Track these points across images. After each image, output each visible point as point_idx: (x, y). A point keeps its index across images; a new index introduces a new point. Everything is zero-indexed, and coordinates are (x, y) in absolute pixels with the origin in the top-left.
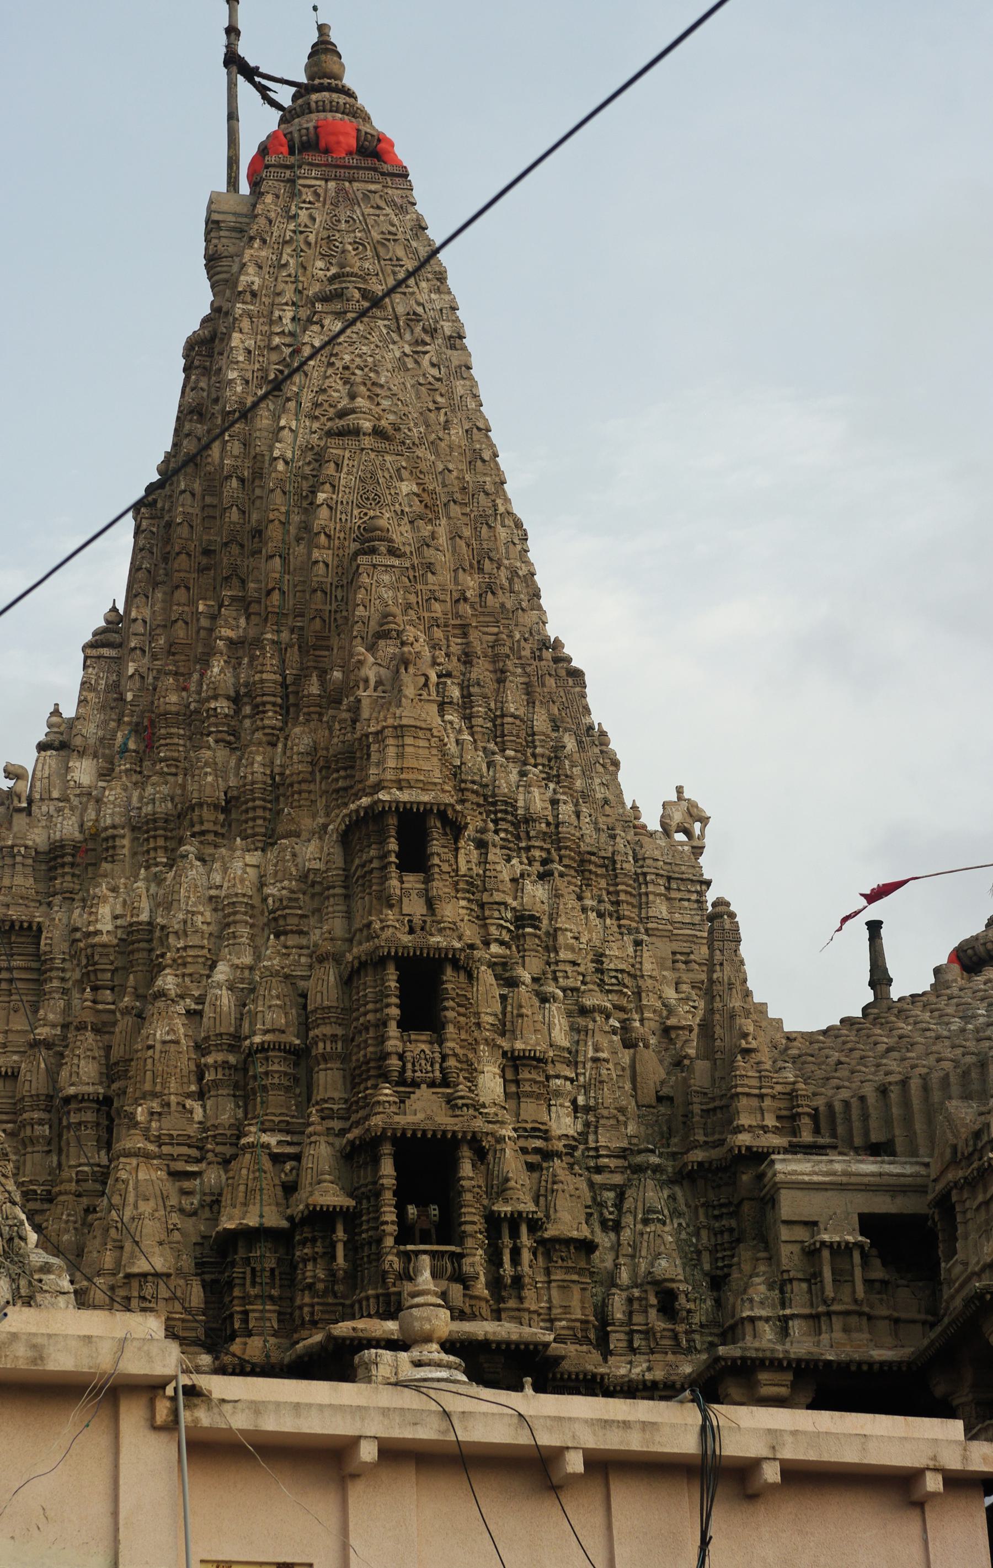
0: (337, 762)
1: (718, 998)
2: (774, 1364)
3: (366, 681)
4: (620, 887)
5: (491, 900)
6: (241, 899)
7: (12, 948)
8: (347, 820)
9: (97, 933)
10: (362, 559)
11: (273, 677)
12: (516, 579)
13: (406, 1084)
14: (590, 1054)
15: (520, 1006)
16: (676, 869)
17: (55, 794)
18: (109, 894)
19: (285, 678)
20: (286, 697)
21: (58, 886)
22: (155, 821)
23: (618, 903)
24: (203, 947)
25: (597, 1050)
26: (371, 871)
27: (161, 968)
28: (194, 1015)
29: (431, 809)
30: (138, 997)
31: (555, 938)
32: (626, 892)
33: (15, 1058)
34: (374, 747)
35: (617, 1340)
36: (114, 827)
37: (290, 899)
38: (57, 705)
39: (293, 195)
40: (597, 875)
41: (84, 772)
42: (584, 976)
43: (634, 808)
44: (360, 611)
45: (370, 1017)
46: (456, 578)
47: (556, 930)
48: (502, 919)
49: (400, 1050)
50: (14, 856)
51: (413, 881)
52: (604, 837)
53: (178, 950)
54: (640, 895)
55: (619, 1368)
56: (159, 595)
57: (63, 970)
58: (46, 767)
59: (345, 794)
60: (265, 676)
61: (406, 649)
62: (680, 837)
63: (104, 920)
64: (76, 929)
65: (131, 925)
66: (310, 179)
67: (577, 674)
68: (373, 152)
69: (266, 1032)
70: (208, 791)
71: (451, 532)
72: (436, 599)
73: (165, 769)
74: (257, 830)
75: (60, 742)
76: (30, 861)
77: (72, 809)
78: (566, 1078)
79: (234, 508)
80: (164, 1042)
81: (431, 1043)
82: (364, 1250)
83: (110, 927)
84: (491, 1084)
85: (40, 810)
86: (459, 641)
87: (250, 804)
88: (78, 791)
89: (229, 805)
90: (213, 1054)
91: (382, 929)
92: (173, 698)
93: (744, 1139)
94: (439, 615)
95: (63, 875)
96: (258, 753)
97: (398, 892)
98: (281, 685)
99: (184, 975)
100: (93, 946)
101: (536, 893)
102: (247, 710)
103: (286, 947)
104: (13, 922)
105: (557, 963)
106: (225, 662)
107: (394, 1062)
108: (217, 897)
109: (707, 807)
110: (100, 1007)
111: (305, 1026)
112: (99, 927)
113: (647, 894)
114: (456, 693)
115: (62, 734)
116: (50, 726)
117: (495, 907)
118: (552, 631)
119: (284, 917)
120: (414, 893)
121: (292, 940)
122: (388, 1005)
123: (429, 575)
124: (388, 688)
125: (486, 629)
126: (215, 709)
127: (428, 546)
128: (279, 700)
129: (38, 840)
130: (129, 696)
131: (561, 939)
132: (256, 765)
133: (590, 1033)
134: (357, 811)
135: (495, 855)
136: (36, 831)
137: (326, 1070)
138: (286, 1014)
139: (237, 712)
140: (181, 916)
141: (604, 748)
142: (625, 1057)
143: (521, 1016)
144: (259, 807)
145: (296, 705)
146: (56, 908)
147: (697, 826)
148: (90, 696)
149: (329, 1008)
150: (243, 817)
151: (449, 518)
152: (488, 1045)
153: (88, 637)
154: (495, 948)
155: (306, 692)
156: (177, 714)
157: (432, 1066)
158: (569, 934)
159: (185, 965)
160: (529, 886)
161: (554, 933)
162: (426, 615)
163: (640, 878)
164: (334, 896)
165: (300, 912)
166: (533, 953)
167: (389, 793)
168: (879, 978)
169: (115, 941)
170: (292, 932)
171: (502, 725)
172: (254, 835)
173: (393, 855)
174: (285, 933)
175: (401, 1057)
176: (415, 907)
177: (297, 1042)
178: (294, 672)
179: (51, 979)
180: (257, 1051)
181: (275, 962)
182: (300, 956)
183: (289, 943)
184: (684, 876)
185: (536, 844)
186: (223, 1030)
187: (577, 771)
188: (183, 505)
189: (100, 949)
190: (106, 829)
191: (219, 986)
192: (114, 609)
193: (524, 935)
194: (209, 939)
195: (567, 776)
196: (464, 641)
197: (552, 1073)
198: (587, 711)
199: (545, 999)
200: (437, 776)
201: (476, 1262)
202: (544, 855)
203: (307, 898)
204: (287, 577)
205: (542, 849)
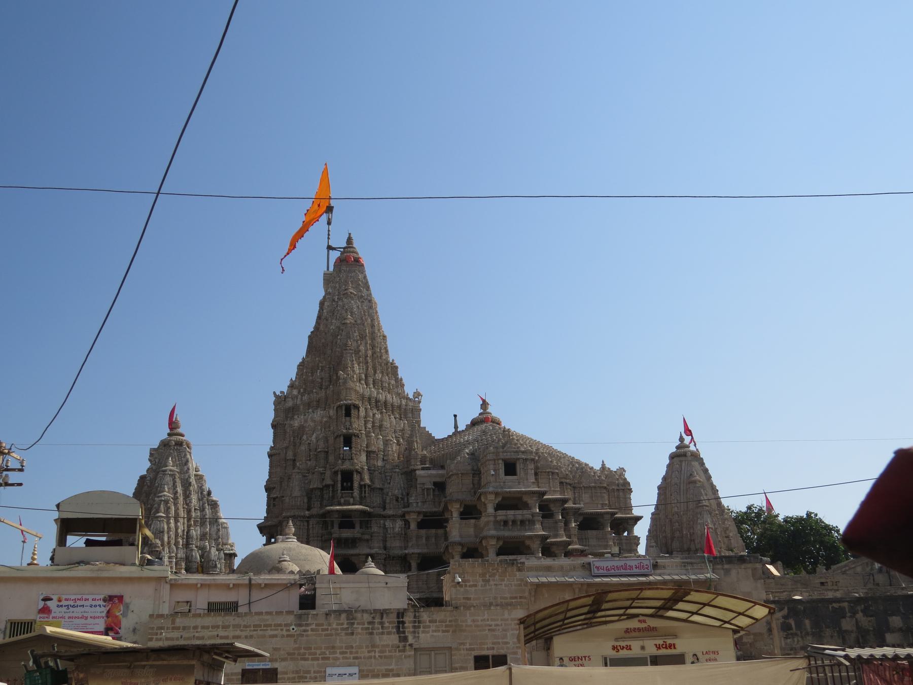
2: (414, 512)
13: (344, 460)
35: (387, 506)
39: (340, 271)
41: (295, 392)
51: (348, 418)
63: (296, 424)
66: (344, 268)
68: (357, 260)
75: (292, 386)
84: (363, 458)
93: (412, 467)
101: (378, 416)
114: (363, 376)
135: (369, 410)
168: (456, 427)
176: (348, 424)
201: (356, 493)
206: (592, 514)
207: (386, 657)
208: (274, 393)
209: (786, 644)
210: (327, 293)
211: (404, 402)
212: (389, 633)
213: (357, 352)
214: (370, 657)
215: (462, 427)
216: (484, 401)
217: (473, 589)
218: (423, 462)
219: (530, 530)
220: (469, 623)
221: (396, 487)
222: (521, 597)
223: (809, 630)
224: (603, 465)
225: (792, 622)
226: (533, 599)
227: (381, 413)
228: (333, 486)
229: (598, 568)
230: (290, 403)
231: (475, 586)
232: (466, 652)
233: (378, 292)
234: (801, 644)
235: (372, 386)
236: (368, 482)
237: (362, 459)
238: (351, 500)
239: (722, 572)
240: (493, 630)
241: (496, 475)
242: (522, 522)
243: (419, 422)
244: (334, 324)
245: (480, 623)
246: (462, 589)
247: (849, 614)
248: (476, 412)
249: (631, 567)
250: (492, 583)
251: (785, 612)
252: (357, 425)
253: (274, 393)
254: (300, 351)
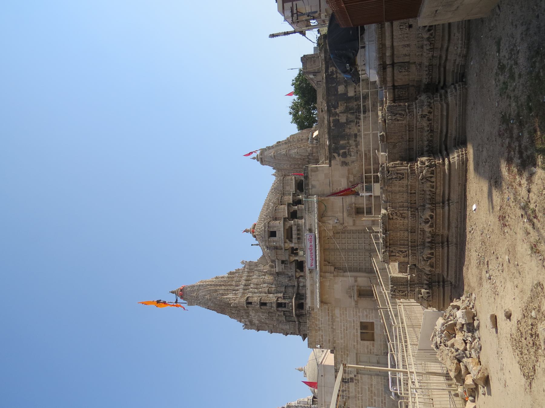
41: (243, 320)
55: (296, 284)
66: (185, 297)
68: (181, 290)
75: (240, 321)
82: (287, 311)
101: (252, 286)
118: (226, 275)
168: (257, 245)
206: (295, 186)
207: (362, 391)
209: (354, 156)
210: (197, 305)
211: (246, 270)
212: (348, 388)
213: (223, 295)
214: (362, 399)
215: (257, 242)
216: (245, 231)
217: (324, 337)
218: (272, 267)
219: (302, 226)
220: (342, 341)
221: (285, 280)
222: (328, 310)
223: (346, 142)
224: (273, 175)
225: (342, 151)
226: (329, 305)
228: (284, 311)
229: (311, 265)
230: (248, 323)
231: (322, 336)
232: (359, 345)
233: (196, 282)
234: (354, 147)
235: (238, 288)
236: (281, 295)
237: (272, 298)
238: (291, 304)
239: (313, 189)
240: (347, 328)
241: (276, 242)
242: (298, 230)
243: (255, 263)
244: (210, 303)
245: (343, 336)
246: (324, 343)
247: (337, 117)
248: (250, 235)
249: (311, 246)
250: (320, 326)
251: (336, 155)
252: (255, 299)
254: (225, 318)
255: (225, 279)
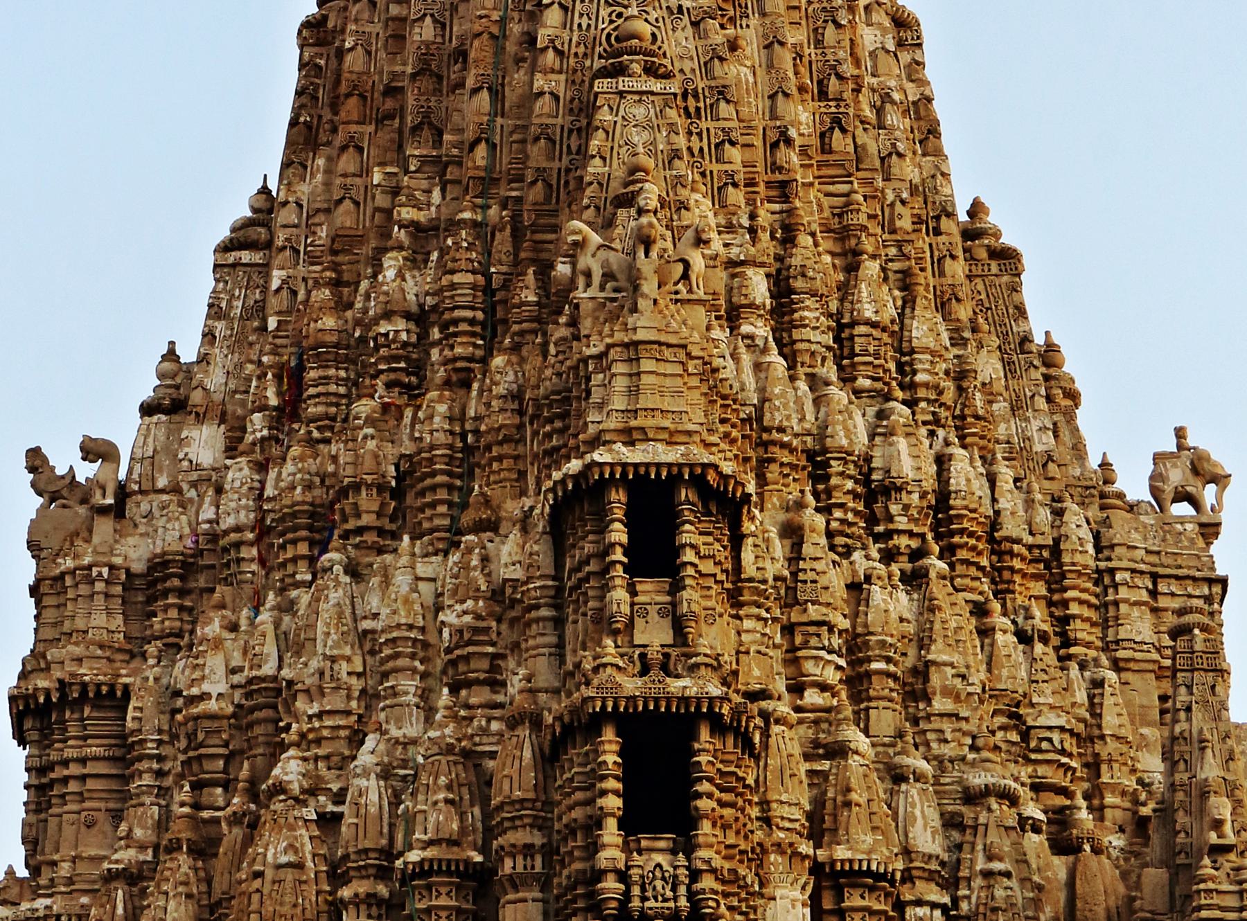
0: (550, 406)
1: (1182, 766)
3: (588, 274)
4: (1070, 594)
5: (804, 619)
6: (407, 634)
7: (85, 727)
8: (550, 496)
9: (205, 696)
10: (601, 85)
11: (470, 278)
12: (888, 106)
14: (980, 865)
15: (849, 790)
16: (1165, 560)
17: (162, 482)
18: (226, 635)
19: (488, 277)
20: (490, 310)
21: (157, 627)
22: (294, 515)
23: (1065, 620)
24: (348, 713)
25: (990, 858)
26: (586, 579)
27: (283, 747)
28: (329, 822)
29: (681, 474)
30: (253, 793)
31: (926, 679)
32: (1081, 602)
33: (85, 900)
34: (597, 379)
36: (238, 529)
37: (476, 630)
38: (172, 343)
40: (1024, 576)
41: (204, 444)
42: (974, 738)
43: (1105, 465)
44: (595, 167)
45: (577, 813)
46: (773, 109)
47: (928, 664)
48: (823, 648)
49: (621, 865)
50: (92, 582)
51: (651, 590)
52: (1043, 516)
53: (310, 717)
54: (1106, 605)
56: (321, 162)
57: (160, 758)
58: (150, 440)
59: (556, 456)
60: (457, 278)
61: (644, 220)
62: (1183, 509)
64: (178, 693)
65: (250, 681)
67: (1008, 258)
69: (431, 843)
70: (369, 464)
71: (765, 36)
72: (733, 144)
73: (316, 434)
74: (437, 522)
75: (171, 403)
76: (118, 589)
77: (182, 505)
78: (934, 906)
79: (428, 19)
80: (279, 867)
81: (674, 852)
83: (222, 687)
85: (138, 507)
86: (777, 207)
87: (428, 482)
88: (194, 476)
89: (404, 486)
90: (355, 883)
91: (596, 670)
92: (329, 322)
94: (738, 166)
95: (166, 609)
96: (440, 400)
97: (626, 609)
98: (484, 292)
99: (317, 758)
100: (197, 718)
101: (892, 605)
102: (436, 334)
103: (468, 707)
104: (84, 686)
105: (928, 717)
106: (405, 259)
107: (611, 885)
108: (373, 632)
109: (1221, 456)
110: (205, 814)
111: (490, 832)
112: (206, 687)
113: (1116, 603)
114: (759, 287)
115: (177, 387)
116: (161, 376)
117: (812, 629)
119: (467, 658)
120: (653, 610)
121: (478, 696)
122: (603, 793)
123: (722, 104)
124: (623, 283)
125: (831, 188)
126: (386, 335)
127: (721, 59)
128: (480, 315)
129: (133, 554)
130: (272, 323)
131: (935, 679)
132: (437, 419)
133: (981, 829)
134: (563, 481)
136: (131, 541)
137: (514, 902)
138: (462, 815)
139: (423, 336)
140: (315, 664)
141: (1053, 371)
142: (1059, 866)
143: (848, 804)
144: (441, 485)
145: (505, 322)
146: (151, 661)
147: (1209, 494)
148: (220, 327)
149: (522, 801)
150: (419, 502)
151: (763, 14)
152: (783, 853)
153: (224, 233)
154: (812, 697)
155: (516, 300)
156: (337, 346)
157: (674, 889)
158: (949, 671)
159: (318, 742)
160: (877, 594)
161: (922, 671)
162: (716, 167)
163: (1103, 578)
164: (537, 620)
165: (490, 649)
166: (882, 704)
167: (610, 451)
169: (230, 709)
170: (478, 682)
171: (852, 338)
172: (432, 531)
173: (619, 550)
174: (469, 684)
175: (623, 876)
176: (654, 635)
177: (479, 858)
178: (504, 269)
179: (141, 773)
180: (414, 876)
181: (447, 731)
182: (489, 721)
183: (473, 701)
184: (1180, 572)
185: (901, 527)
186: (368, 844)
187: (1000, 407)
188: (356, 21)
189: (207, 724)
190: (226, 533)
191: (366, 774)
192: (265, 190)
193: (869, 675)
194: (359, 699)
195: (977, 417)
196: (785, 206)
197: (908, 897)
198: (1021, 312)
199: (897, 776)
200: (695, 418)
202: (914, 544)
203: (504, 627)
204: (499, 120)
205: (911, 534)
208: (36, 461)
227: (915, 580)
230: (165, 532)
235: (829, 371)
253: (36, 461)
255: (909, 170)
